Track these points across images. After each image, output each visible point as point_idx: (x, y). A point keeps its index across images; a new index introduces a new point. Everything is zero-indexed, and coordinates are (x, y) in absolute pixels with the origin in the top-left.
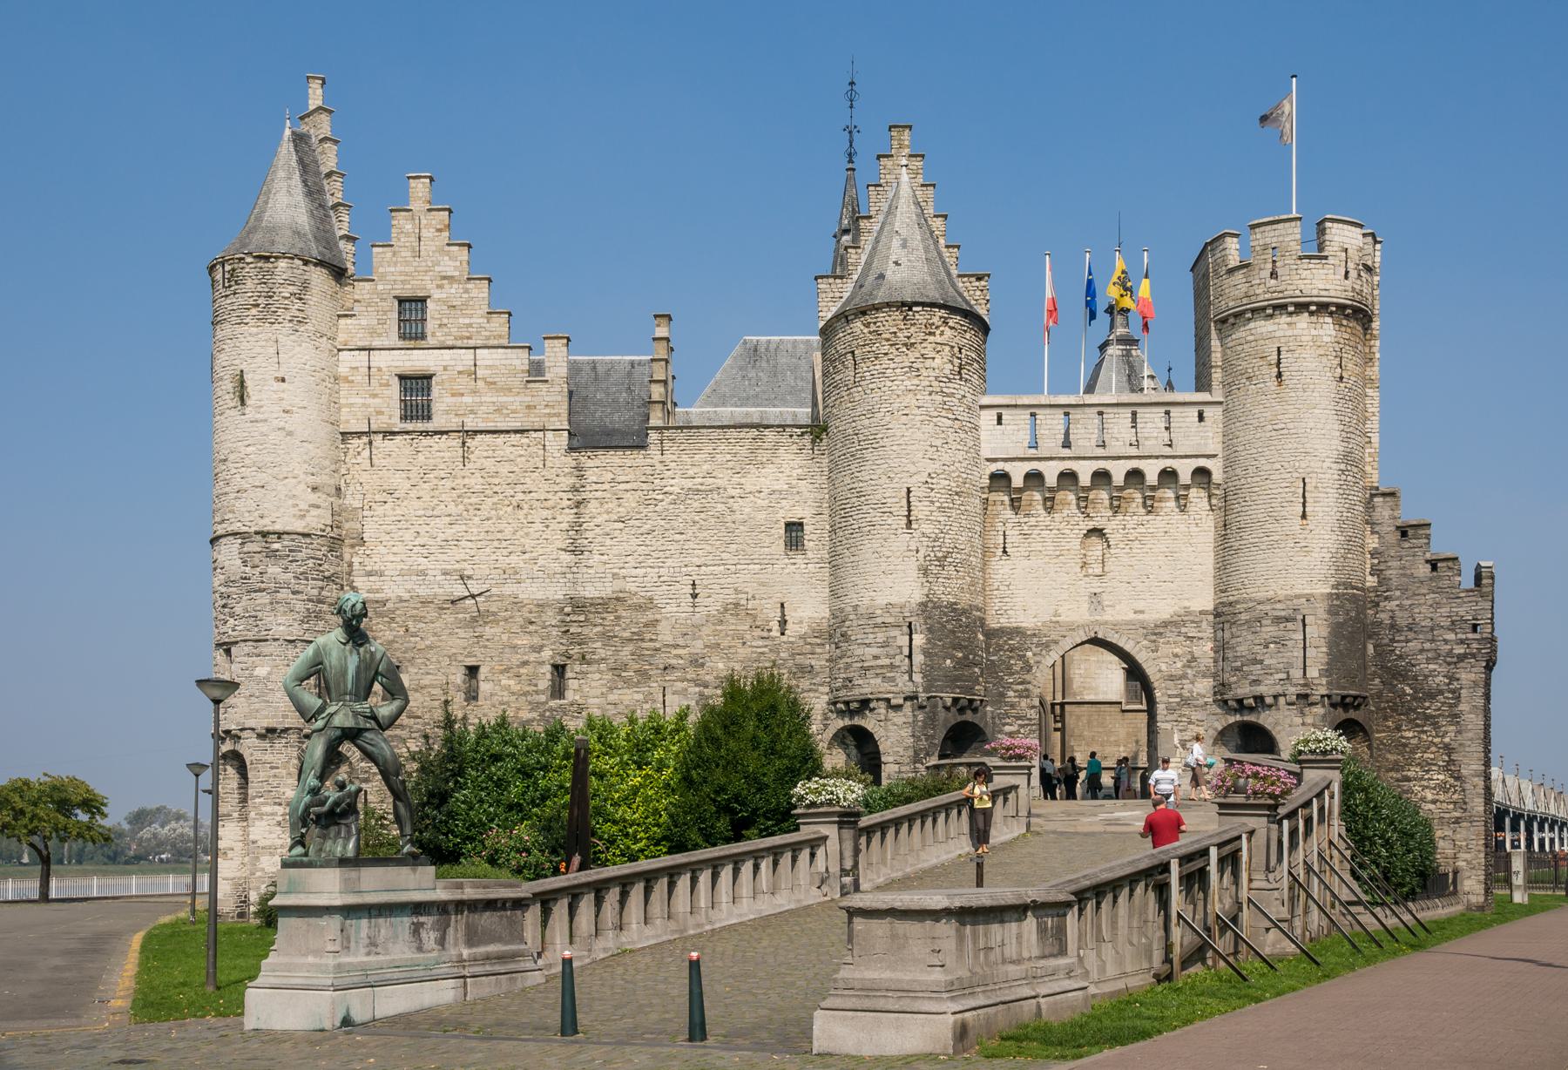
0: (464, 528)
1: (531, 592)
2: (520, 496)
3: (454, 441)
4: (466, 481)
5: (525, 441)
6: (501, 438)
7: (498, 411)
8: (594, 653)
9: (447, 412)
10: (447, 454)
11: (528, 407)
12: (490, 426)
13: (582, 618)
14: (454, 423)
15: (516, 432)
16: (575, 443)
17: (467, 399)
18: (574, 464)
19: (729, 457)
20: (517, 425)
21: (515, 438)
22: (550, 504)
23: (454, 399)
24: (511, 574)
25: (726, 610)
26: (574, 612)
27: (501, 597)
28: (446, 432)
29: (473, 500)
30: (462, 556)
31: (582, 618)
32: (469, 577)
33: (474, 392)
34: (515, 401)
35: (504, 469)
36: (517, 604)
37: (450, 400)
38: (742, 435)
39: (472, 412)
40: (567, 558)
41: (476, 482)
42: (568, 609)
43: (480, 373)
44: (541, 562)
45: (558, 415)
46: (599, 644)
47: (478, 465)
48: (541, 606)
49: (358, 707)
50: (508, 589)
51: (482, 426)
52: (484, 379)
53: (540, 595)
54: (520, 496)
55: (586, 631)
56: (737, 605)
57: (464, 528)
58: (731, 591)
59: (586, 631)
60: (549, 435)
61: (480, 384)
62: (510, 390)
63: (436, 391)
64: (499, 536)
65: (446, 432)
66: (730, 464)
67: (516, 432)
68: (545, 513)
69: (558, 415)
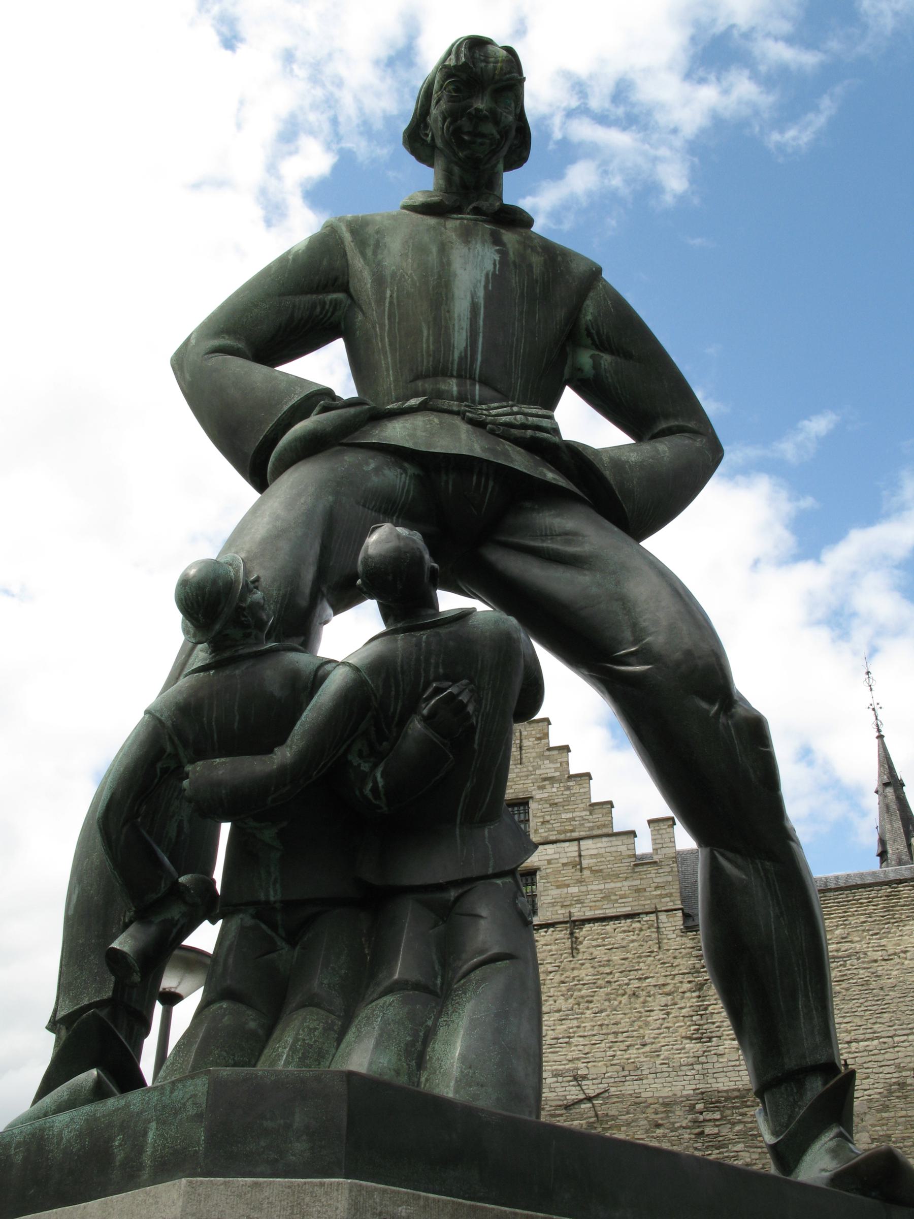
0: (575, 1023)
1: (656, 1088)
2: (636, 984)
3: (561, 934)
4: (576, 973)
5: (637, 925)
6: (610, 927)
7: (606, 897)
8: (736, 1157)
9: (553, 904)
10: (554, 947)
11: (638, 891)
12: (599, 913)
13: (717, 1116)
14: (560, 914)
15: (627, 916)
16: (690, 923)
17: (574, 890)
18: (690, 944)
19: (863, 918)
20: (627, 910)
21: (625, 924)
22: (668, 989)
23: (559, 891)
24: (633, 1071)
25: (890, 1092)
26: (707, 1109)
27: (621, 1097)
28: (552, 925)
29: (583, 992)
30: (576, 1054)
31: (717, 1116)
32: (584, 1077)
33: (580, 882)
34: (623, 886)
35: (616, 957)
36: (639, 1103)
37: (555, 892)
38: (873, 894)
39: (579, 902)
40: (693, 1047)
41: (586, 973)
42: (700, 1106)
43: (585, 863)
44: (664, 1054)
45: (670, 895)
46: (740, 1147)
47: (586, 956)
48: (668, 1105)
49: (500, 412)
50: (629, 1088)
51: (589, 914)
52: (590, 868)
53: (666, 1092)
54: (636, 984)
55: (725, 1130)
56: (902, 1085)
57: (575, 1023)
58: (892, 1069)
59: (725, 1130)
60: (663, 917)
61: (586, 873)
62: (617, 876)
63: (540, 883)
64: (615, 1029)
65: (552, 925)
66: (866, 926)
67: (627, 916)
68: (664, 1000)
69: (670, 895)
